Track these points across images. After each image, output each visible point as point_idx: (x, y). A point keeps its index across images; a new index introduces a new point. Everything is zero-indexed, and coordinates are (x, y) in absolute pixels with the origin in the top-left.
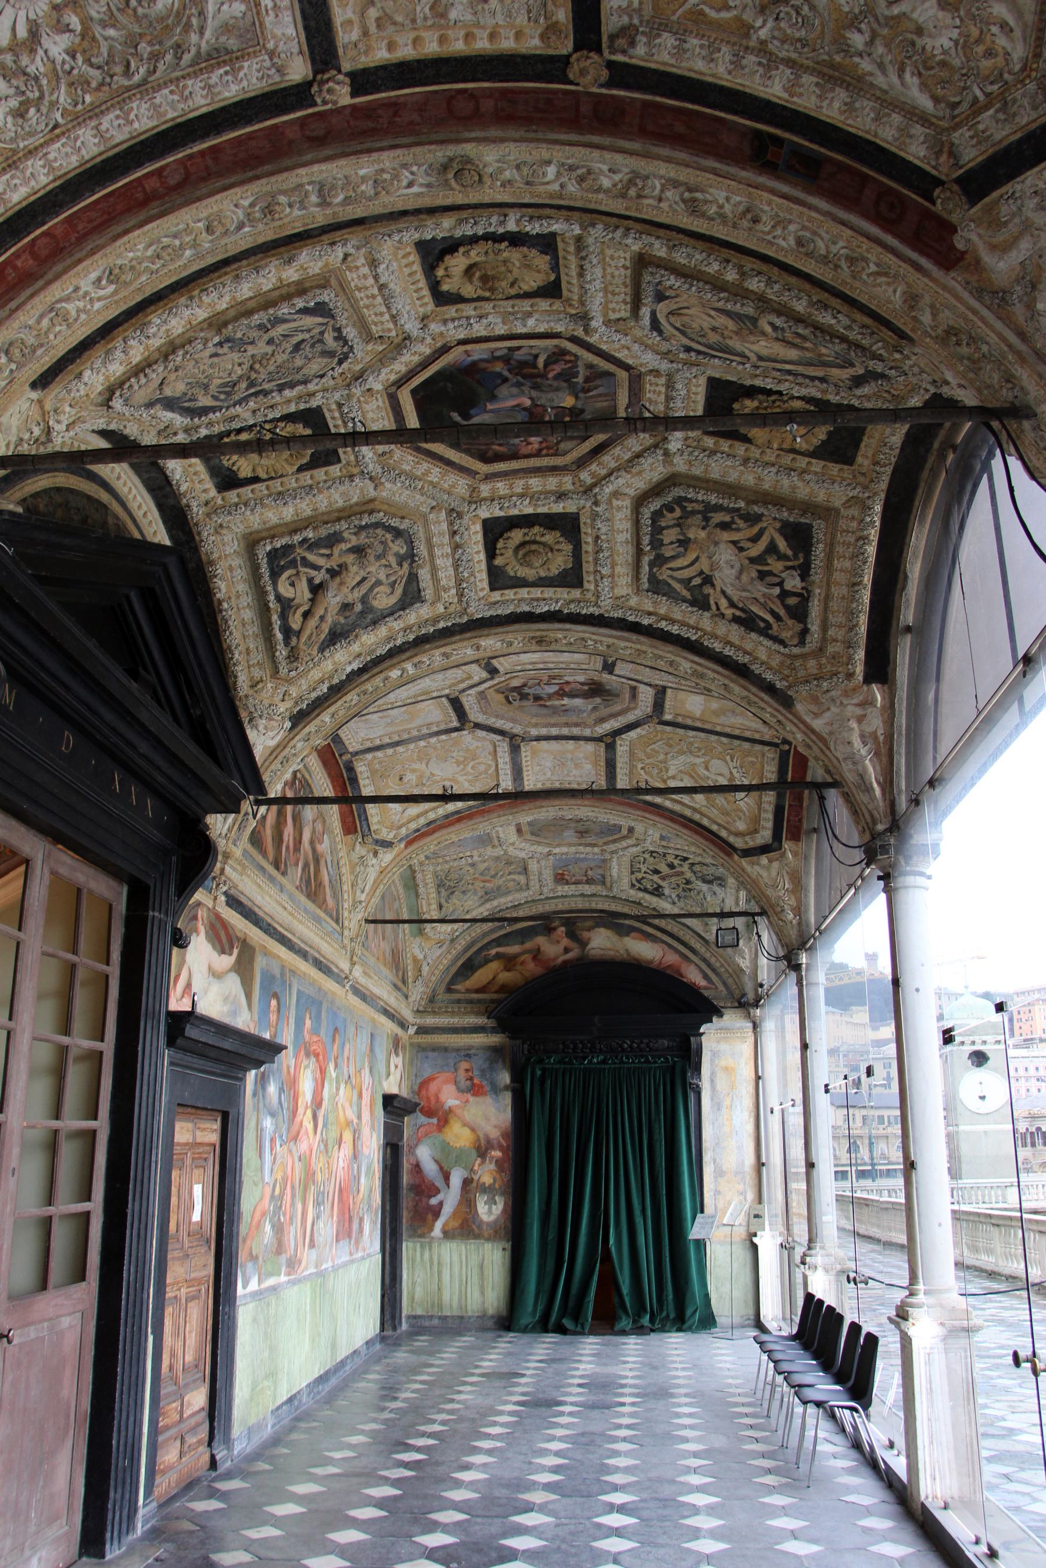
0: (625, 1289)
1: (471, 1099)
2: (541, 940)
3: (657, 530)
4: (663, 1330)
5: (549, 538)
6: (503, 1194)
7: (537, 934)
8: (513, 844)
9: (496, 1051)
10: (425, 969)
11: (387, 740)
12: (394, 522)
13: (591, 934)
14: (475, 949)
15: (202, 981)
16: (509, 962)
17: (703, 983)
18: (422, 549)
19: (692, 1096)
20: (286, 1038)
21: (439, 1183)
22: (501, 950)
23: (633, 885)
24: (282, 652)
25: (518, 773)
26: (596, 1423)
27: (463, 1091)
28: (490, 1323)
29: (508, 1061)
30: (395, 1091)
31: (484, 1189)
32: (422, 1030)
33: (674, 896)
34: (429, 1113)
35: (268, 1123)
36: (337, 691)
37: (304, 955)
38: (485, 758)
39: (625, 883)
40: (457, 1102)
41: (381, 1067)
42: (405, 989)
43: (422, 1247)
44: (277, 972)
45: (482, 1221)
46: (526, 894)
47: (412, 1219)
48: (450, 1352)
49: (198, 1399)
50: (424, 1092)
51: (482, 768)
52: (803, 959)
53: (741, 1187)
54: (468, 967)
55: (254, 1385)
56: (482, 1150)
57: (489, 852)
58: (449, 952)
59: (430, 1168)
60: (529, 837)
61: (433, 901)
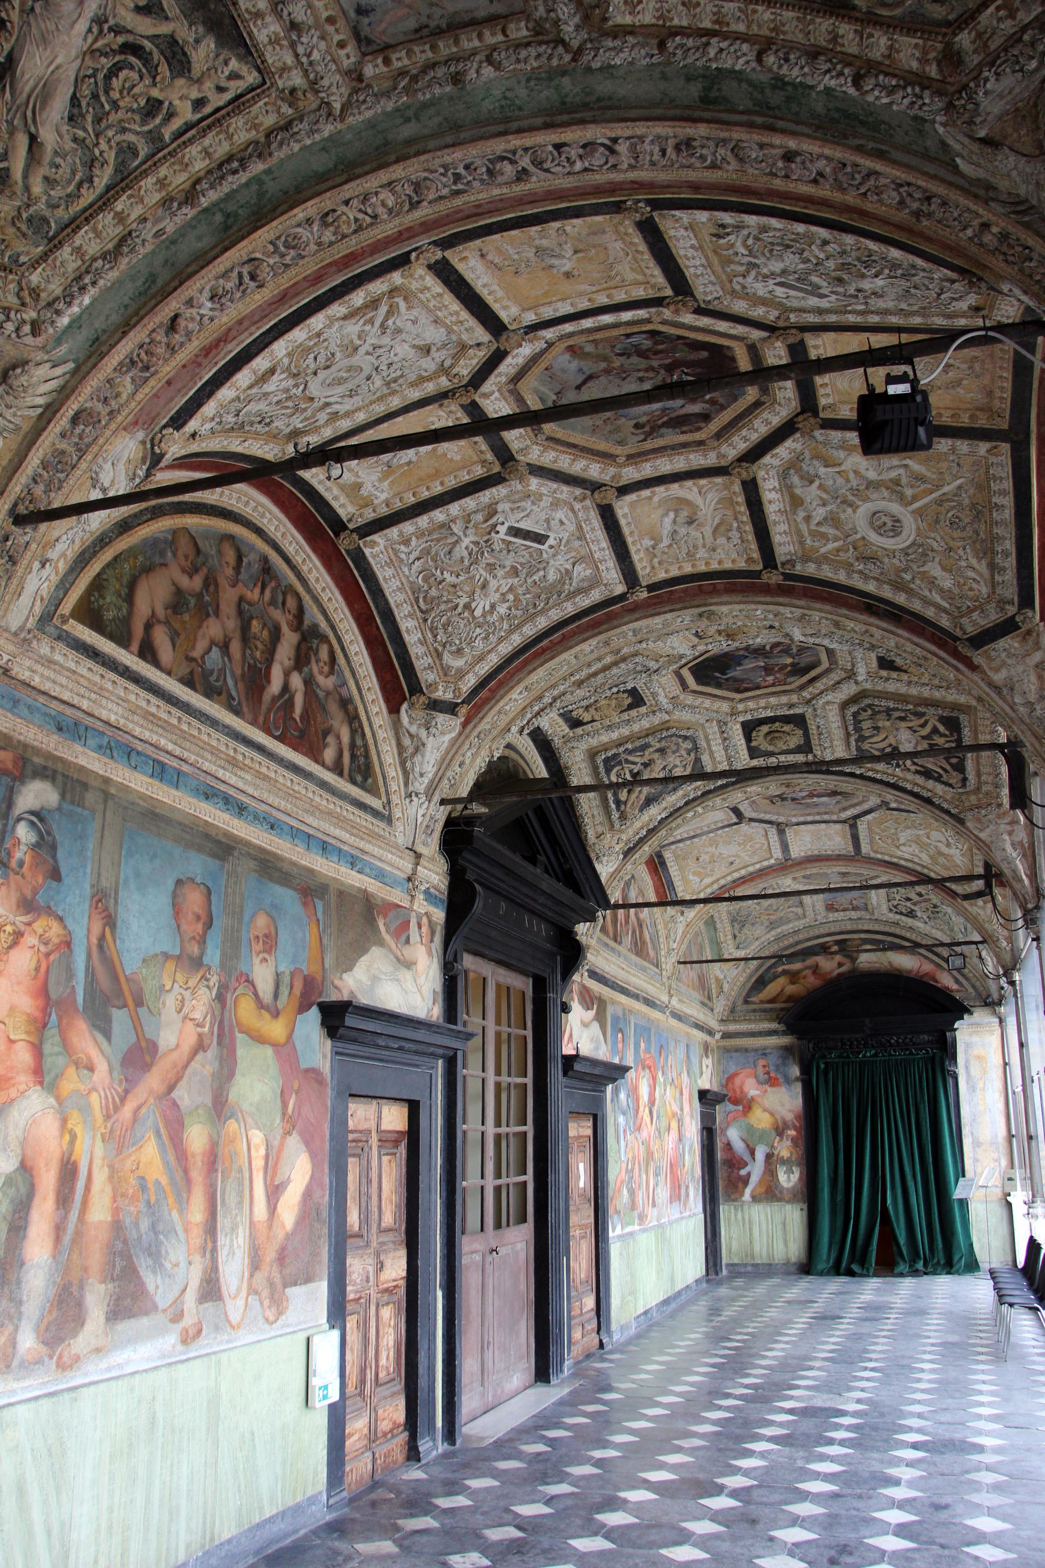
0: (902, 1240)
3: (857, 722)
4: (934, 1273)
5: (787, 728)
9: (787, 1049)
10: (726, 987)
12: (683, 733)
15: (580, 1034)
16: (793, 977)
17: (955, 987)
18: (702, 743)
19: (950, 1081)
20: (629, 1061)
21: (747, 1157)
24: (615, 815)
25: (785, 847)
26: (866, 1328)
28: (793, 1269)
30: (707, 1086)
31: (783, 1162)
32: (726, 1036)
34: (736, 1102)
35: (621, 1119)
36: (652, 832)
37: (636, 997)
38: (760, 839)
39: (884, 908)
41: (696, 1069)
44: (620, 1014)
47: (727, 1187)
48: (761, 1288)
49: (590, 1302)
52: (1017, 977)
53: (995, 1155)
54: (760, 983)
55: (623, 1298)
59: (739, 1146)
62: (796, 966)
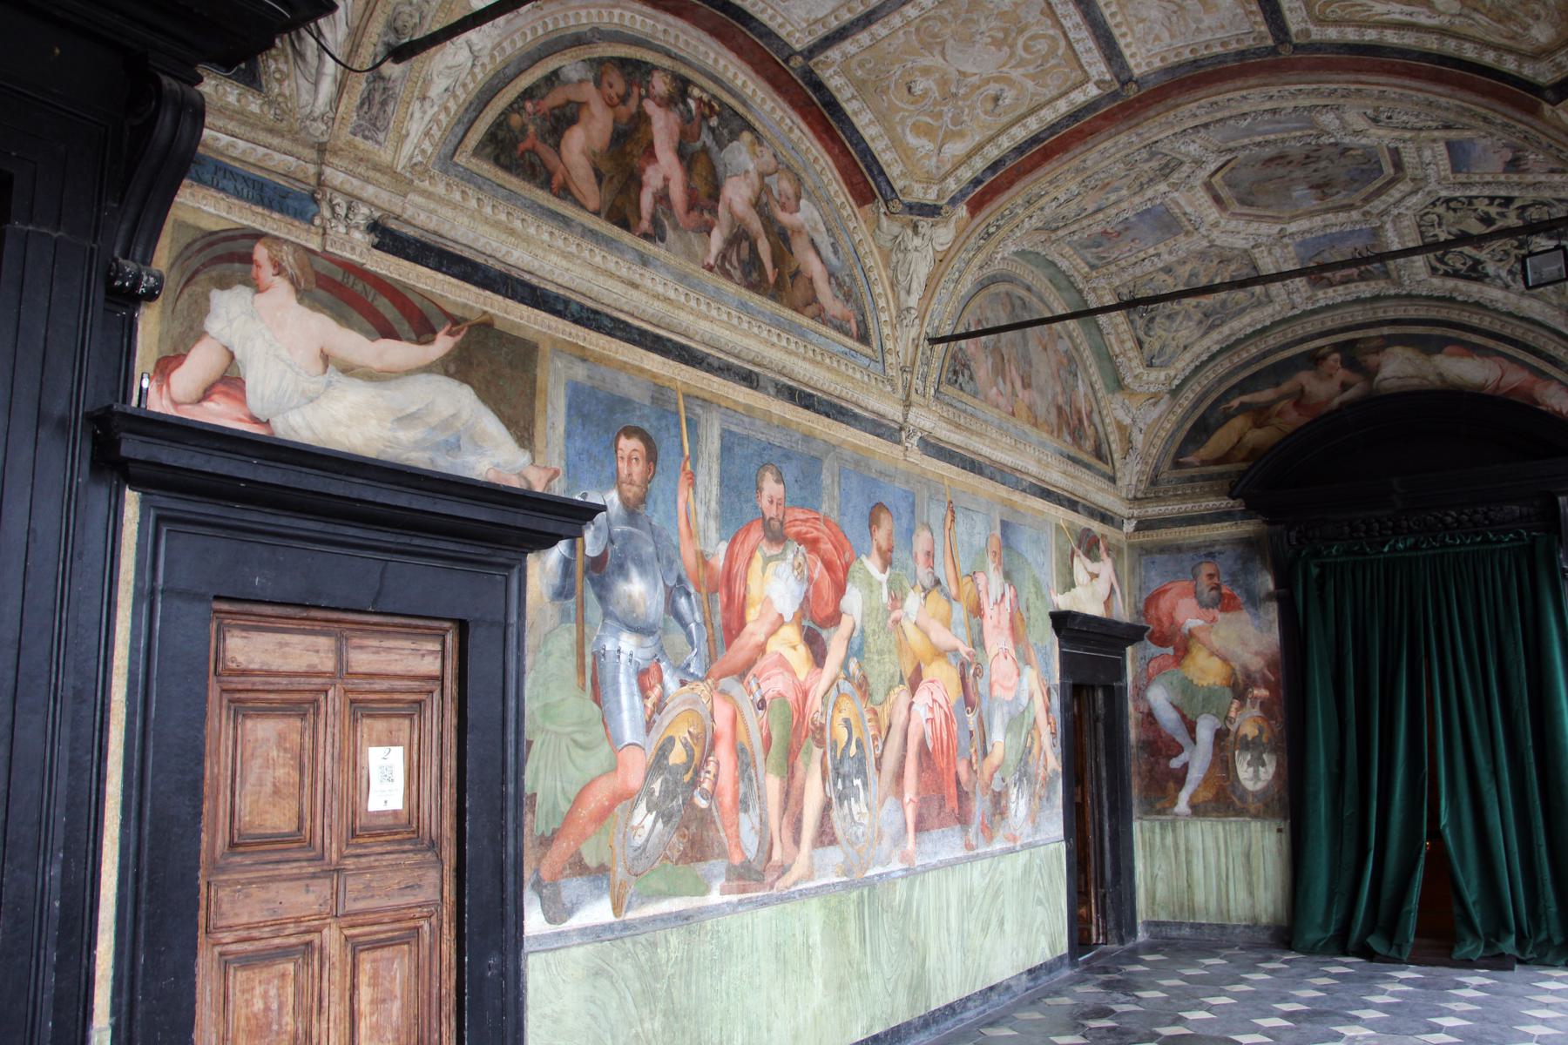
0: (1471, 893)
1: (1220, 616)
2: (1305, 378)
6: (1274, 750)
7: (1298, 369)
8: (1216, 225)
9: (1249, 545)
10: (1138, 439)
11: (847, 17)
13: (1382, 358)
14: (1209, 401)
16: (1260, 415)
21: (1181, 737)
22: (1246, 398)
23: (1434, 270)
27: (1207, 607)
28: (1264, 937)
31: (1246, 744)
32: (1144, 525)
33: (1503, 274)
34: (1162, 641)
37: (749, 379)
40: (1200, 622)
42: (1107, 469)
43: (1163, 828)
45: (1245, 790)
46: (1269, 310)
50: (1152, 612)
51: (1042, 46)
54: (1201, 430)
56: (1239, 688)
57: (1183, 244)
58: (1172, 411)
59: (1168, 717)
60: (1237, 208)
61: (1126, 336)
62: (1266, 395)
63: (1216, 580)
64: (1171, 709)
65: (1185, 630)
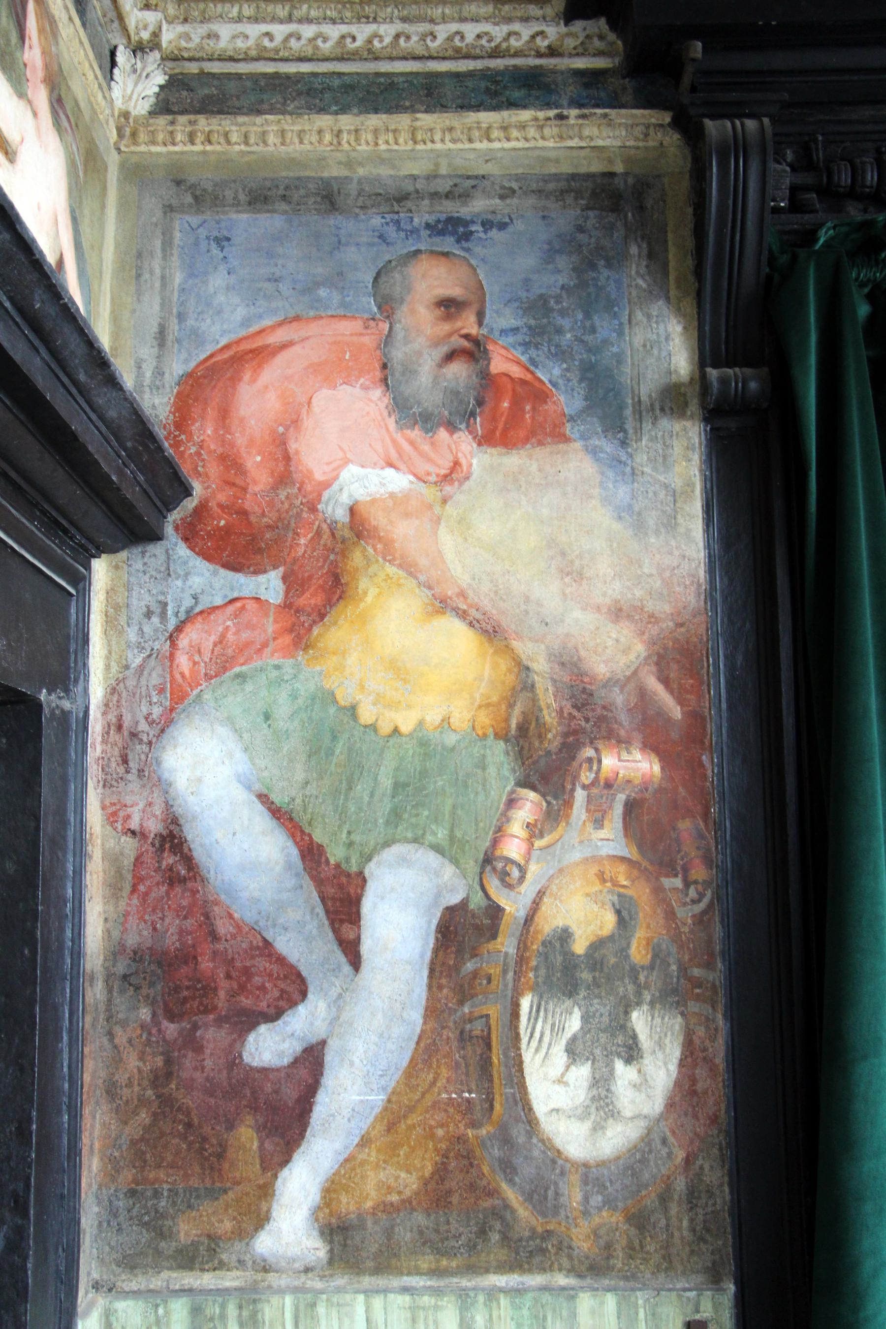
1: (480, 461)
6: (673, 996)
21: (301, 939)
27: (427, 421)
29: (677, 258)
31: (564, 971)
32: (192, 93)
34: (236, 544)
40: (397, 481)
45: (554, 1157)
47: (140, 1153)
63: (468, 324)
64: (262, 820)
65: (335, 508)
